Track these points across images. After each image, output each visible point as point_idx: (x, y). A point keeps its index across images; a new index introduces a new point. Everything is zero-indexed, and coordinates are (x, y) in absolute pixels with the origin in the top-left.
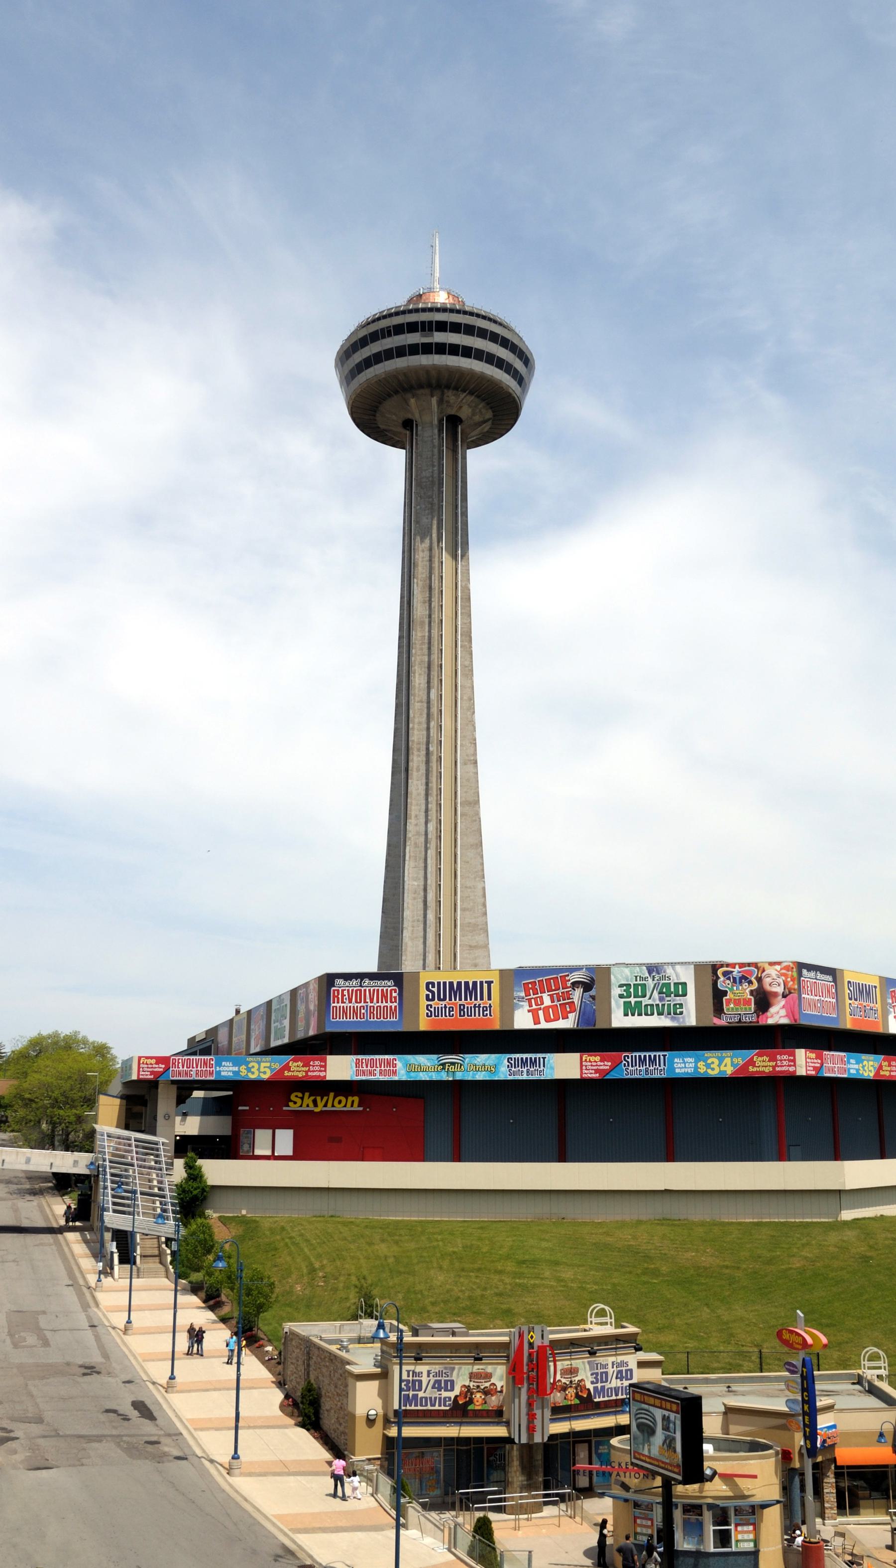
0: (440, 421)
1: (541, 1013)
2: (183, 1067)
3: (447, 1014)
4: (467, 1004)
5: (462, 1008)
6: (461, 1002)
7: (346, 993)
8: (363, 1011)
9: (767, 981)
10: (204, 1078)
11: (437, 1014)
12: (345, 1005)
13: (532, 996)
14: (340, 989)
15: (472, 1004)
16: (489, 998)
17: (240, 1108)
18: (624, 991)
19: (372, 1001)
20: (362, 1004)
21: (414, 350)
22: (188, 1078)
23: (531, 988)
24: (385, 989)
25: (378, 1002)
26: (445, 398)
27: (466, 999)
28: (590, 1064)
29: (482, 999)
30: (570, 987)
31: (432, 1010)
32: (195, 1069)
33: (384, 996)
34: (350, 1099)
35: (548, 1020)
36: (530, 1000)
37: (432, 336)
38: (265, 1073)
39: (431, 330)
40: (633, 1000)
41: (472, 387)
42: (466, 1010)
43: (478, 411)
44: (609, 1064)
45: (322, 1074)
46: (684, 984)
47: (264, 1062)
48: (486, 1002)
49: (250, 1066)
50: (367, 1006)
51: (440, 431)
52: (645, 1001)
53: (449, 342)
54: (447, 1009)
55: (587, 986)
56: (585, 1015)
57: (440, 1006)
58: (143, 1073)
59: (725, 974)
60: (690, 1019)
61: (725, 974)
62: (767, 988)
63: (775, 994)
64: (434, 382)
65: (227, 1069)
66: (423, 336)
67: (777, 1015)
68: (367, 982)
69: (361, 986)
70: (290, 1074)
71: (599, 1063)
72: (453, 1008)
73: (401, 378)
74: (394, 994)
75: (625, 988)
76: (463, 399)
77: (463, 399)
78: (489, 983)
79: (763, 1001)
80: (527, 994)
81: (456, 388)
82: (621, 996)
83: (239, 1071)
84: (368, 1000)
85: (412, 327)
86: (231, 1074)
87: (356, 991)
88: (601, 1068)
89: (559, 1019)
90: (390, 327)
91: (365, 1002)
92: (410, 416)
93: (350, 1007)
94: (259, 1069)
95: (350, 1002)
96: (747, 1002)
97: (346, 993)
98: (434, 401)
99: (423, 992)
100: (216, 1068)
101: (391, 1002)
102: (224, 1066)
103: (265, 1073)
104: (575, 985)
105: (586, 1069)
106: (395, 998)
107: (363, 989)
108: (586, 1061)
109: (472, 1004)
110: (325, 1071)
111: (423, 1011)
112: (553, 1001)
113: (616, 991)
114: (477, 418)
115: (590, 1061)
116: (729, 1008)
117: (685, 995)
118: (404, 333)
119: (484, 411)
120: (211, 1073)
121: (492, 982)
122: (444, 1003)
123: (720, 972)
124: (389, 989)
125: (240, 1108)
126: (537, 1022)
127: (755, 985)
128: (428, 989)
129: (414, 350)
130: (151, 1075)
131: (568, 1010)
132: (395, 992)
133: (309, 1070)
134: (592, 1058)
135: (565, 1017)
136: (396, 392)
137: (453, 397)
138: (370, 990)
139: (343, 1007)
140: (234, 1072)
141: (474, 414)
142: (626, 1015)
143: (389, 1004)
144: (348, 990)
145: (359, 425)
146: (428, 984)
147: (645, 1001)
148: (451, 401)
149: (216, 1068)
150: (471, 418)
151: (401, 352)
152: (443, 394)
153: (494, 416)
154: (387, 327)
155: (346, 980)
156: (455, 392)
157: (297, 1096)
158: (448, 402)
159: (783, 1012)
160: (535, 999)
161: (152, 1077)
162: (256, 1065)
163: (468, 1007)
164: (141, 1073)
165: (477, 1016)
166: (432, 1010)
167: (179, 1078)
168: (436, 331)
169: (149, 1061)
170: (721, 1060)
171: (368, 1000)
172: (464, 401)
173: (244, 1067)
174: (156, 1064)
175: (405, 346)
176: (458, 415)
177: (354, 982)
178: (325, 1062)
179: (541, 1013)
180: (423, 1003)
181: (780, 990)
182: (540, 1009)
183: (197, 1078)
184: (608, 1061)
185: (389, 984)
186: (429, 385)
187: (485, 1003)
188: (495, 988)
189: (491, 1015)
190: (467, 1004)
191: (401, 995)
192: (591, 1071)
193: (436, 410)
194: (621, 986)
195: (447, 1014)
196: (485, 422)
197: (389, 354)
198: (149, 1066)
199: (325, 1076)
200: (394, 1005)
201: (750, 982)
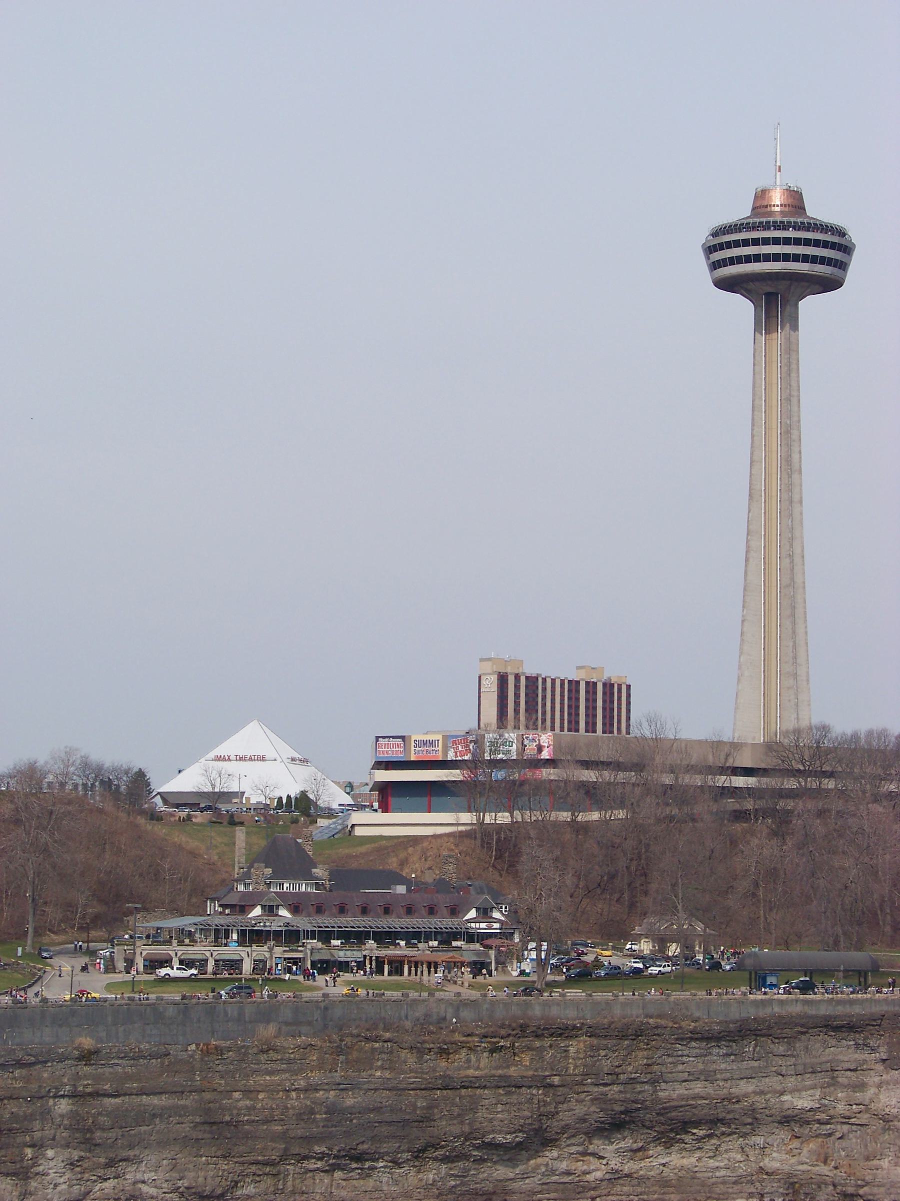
9: (542, 741)
48: (437, 748)
55: (475, 742)
62: (542, 744)
63: (545, 746)
67: (545, 755)
78: (438, 740)
79: (540, 749)
82: (489, 746)
99: (413, 744)
104: (471, 741)
111: (413, 752)
117: (512, 746)
126: (456, 756)
127: (537, 743)
159: (547, 754)
180: (413, 748)
181: (546, 745)
201: (536, 741)
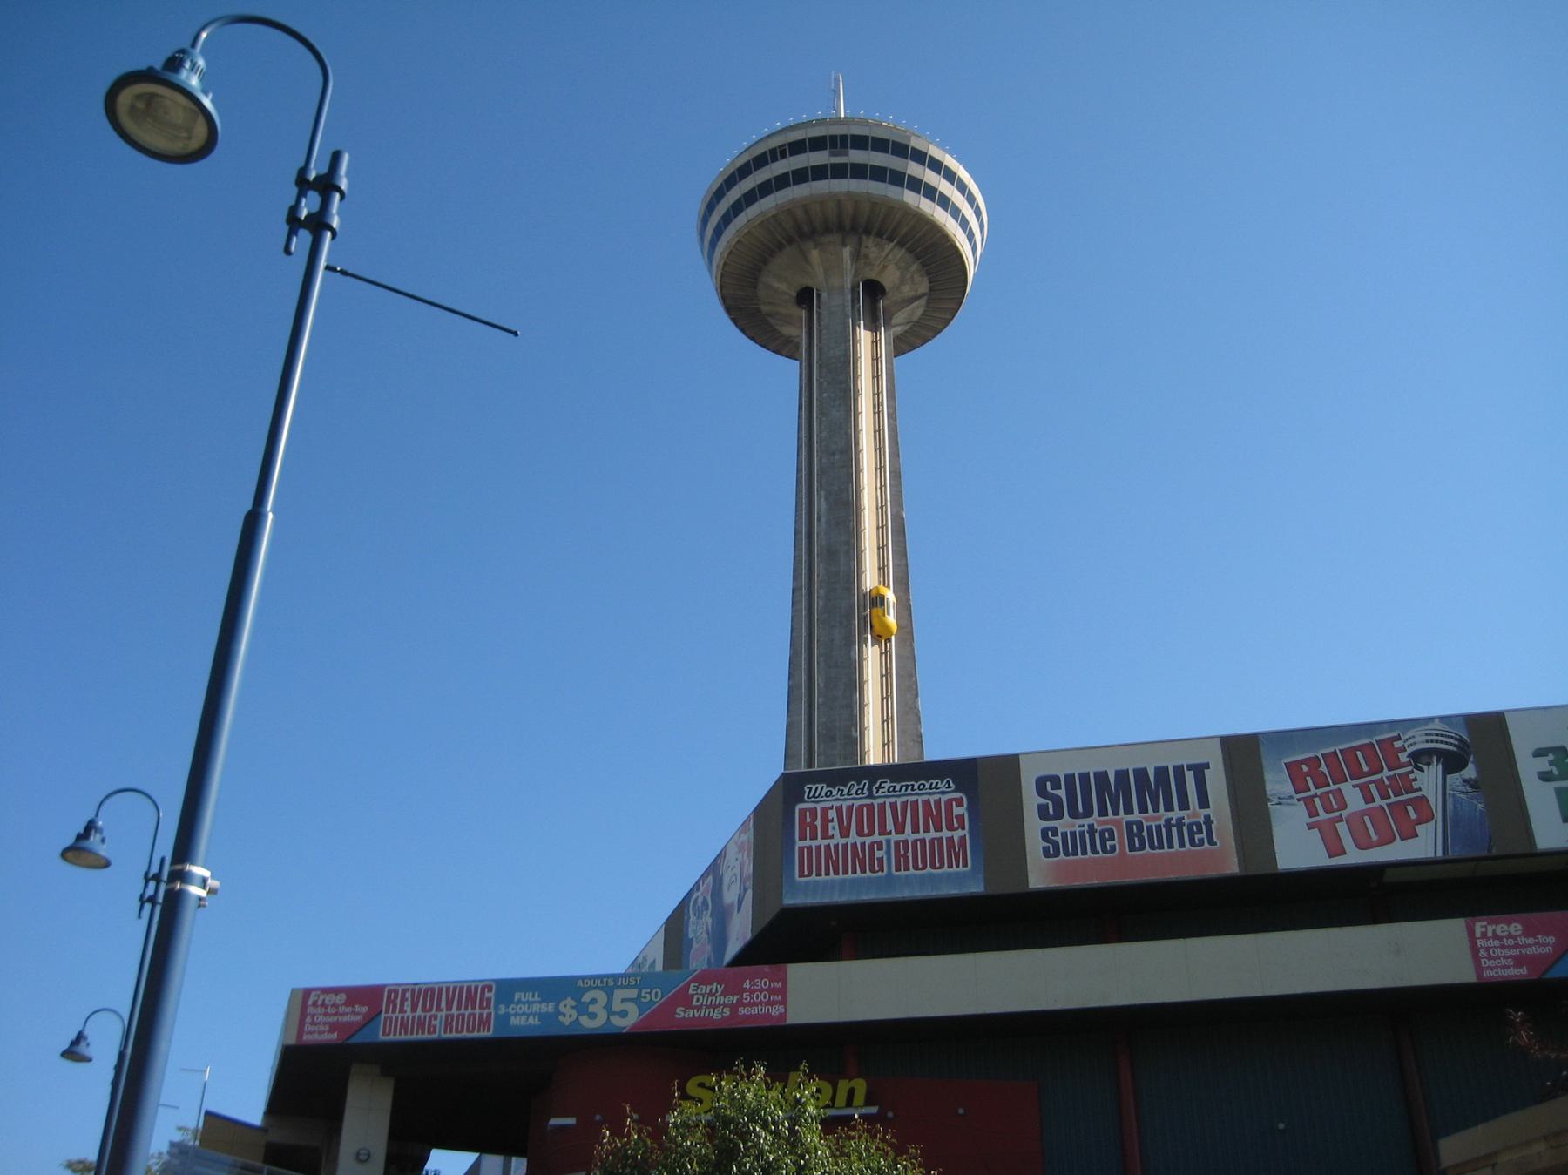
0: (854, 289)
1: (1342, 828)
2: (414, 1009)
3: (1099, 847)
4: (1147, 819)
5: (1134, 831)
6: (1130, 818)
7: (832, 814)
8: (878, 854)
10: (465, 1034)
11: (1072, 844)
12: (832, 842)
13: (1313, 791)
14: (819, 807)
15: (1159, 818)
16: (1204, 802)
17: (554, 1121)
18: (1551, 763)
19: (900, 829)
20: (876, 837)
21: (819, 173)
22: (426, 1036)
23: (1308, 774)
24: (932, 799)
25: (915, 830)
26: (863, 251)
27: (1143, 810)
28: (1497, 943)
29: (1184, 805)
30: (1409, 764)
31: (1059, 839)
32: (444, 1013)
33: (932, 817)
34: (844, 1086)
35: (1363, 845)
36: (1309, 802)
37: (846, 154)
38: (624, 1014)
39: (844, 145)
41: (903, 232)
42: (1145, 834)
43: (909, 276)
44: (1551, 940)
45: (775, 1011)
47: (622, 987)
48: (1194, 813)
49: (586, 998)
50: (888, 842)
51: (855, 300)
53: (871, 163)
54: (1097, 836)
57: (1078, 830)
58: (311, 1028)
64: (847, 223)
65: (525, 1008)
66: (832, 155)
69: (871, 796)
70: (690, 1013)
71: (1522, 941)
72: (1111, 832)
73: (800, 214)
74: (957, 811)
75: (1551, 757)
76: (889, 253)
77: (889, 253)
81: (879, 235)
83: (558, 1013)
84: (890, 826)
85: (817, 144)
86: (537, 1022)
87: (861, 807)
88: (1530, 951)
89: (1392, 840)
90: (784, 145)
91: (883, 832)
92: (809, 283)
93: (845, 846)
94: (608, 1007)
95: (845, 833)
97: (832, 814)
98: (847, 252)
99: (1031, 801)
100: (497, 1008)
101: (950, 828)
102: (519, 1001)
103: (624, 1014)
104: (1419, 758)
105: (1490, 958)
106: (960, 818)
107: (876, 802)
108: (1484, 935)
109: (1159, 818)
110: (784, 1002)
111: (1034, 843)
112: (1369, 799)
114: (907, 291)
115: (1495, 936)
118: (805, 152)
119: (917, 278)
120: (484, 1023)
121: (1207, 766)
122: (1086, 821)
124: (944, 798)
125: (554, 1121)
126: (1335, 849)
129: (819, 173)
130: (331, 1031)
131: (1413, 816)
132: (960, 803)
133: (740, 1003)
134: (1501, 929)
136: (791, 241)
137: (874, 249)
138: (893, 806)
139: (828, 847)
140: (542, 1016)
141: (902, 281)
143: (945, 834)
144: (839, 809)
145: (728, 310)
148: (872, 256)
149: (497, 1008)
150: (898, 288)
151: (800, 176)
152: (860, 245)
153: (931, 289)
154: (780, 147)
155: (832, 784)
156: (878, 239)
157: (701, 1085)
158: (866, 257)
160: (1324, 798)
161: (334, 1036)
162: (602, 997)
163: (1150, 829)
164: (308, 1028)
166: (1059, 839)
167: (403, 1037)
168: (852, 148)
169: (329, 998)
171: (890, 826)
172: (890, 256)
173: (570, 1002)
174: (347, 1004)
175: (807, 168)
176: (880, 280)
178: (784, 981)
180: (1033, 824)
182: (1340, 819)
183: (448, 1035)
184: (1547, 934)
185: (942, 786)
186: (841, 228)
187: (1195, 815)
189: (1211, 842)
190: (1147, 819)
192: (1503, 962)
193: (849, 266)
194: (1539, 753)
195: (1099, 847)
196: (916, 298)
197: (782, 182)
198: (330, 1010)
199: (783, 1016)
200: (957, 834)
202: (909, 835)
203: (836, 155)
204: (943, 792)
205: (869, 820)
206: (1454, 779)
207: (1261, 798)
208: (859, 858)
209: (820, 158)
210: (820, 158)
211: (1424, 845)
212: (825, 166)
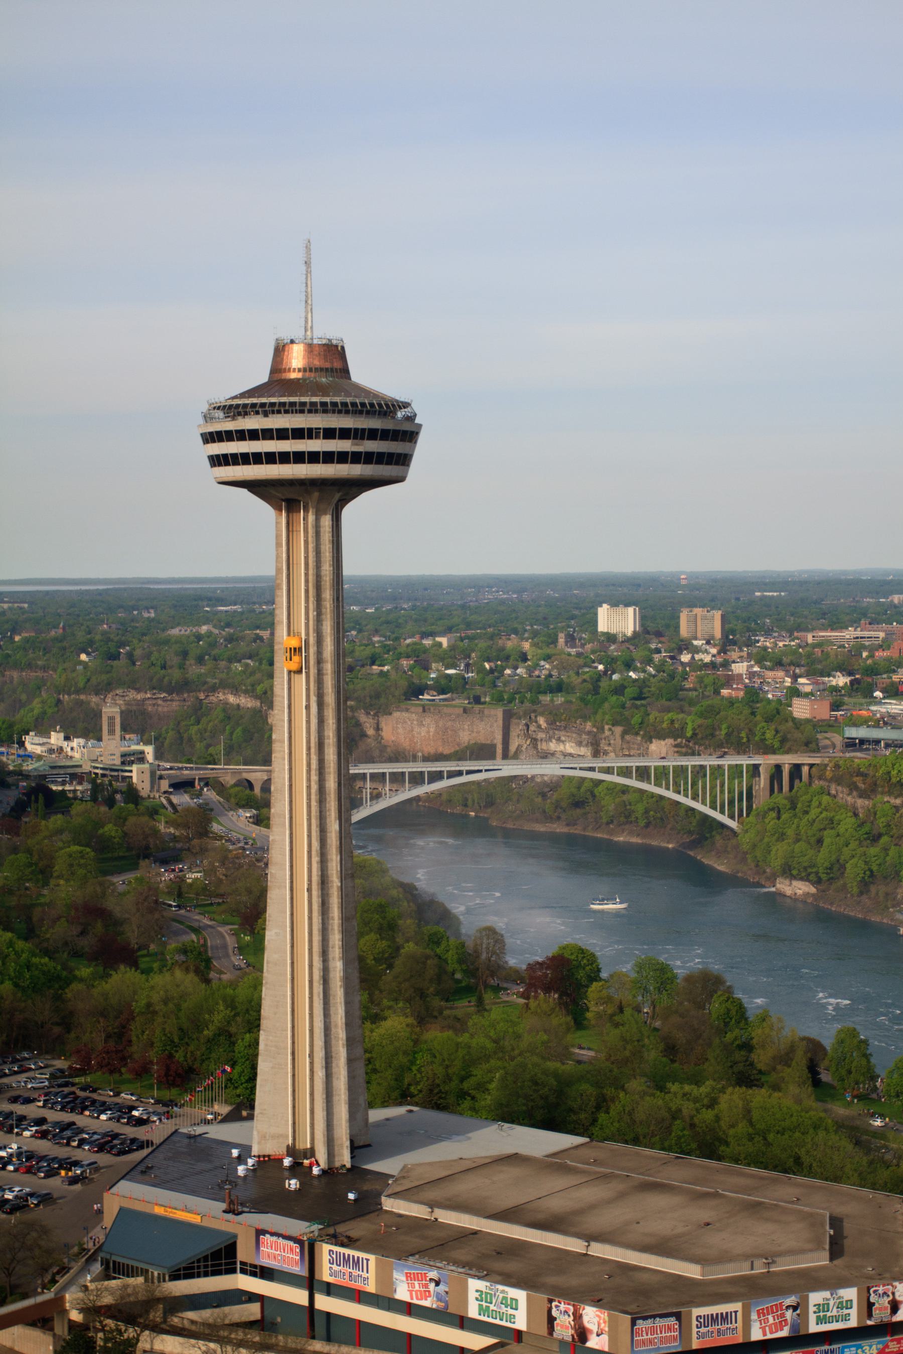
1: (767, 1328)
19: (661, 1332)
33: (669, 1329)
35: (771, 1333)
39: (362, 438)
40: (821, 1314)
46: (851, 1301)
48: (734, 1325)
52: (829, 1314)
56: (794, 1327)
59: (875, 1291)
60: (853, 1323)
61: (875, 1291)
68: (658, 1319)
78: (736, 1312)
80: (759, 1317)
82: (815, 1312)
95: (647, 1334)
96: (886, 1308)
99: (694, 1323)
104: (788, 1307)
111: (694, 1335)
113: (812, 1309)
116: (876, 1312)
123: (871, 1291)
127: (891, 1298)
128: (697, 1320)
135: (782, 1330)
142: (817, 1324)
146: (697, 1317)
147: (829, 1314)
154: (316, 429)
165: (729, 1335)
170: (871, 1346)
177: (650, 1321)
179: (767, 1328)
180: (695, 1330)
188: (739, 1315)
191: (680, 1326)
201: (888, 1296)
202: (663, 1335)
203: (357, 445)
204: (672, 1321)
205: (653, 1330)
206: (795, 1313)
207: (750, 1320)
208: (651, 1342)
209: (345, 445)
210: (345, 445)
211: (784, 1333)
212: (347, 453)
